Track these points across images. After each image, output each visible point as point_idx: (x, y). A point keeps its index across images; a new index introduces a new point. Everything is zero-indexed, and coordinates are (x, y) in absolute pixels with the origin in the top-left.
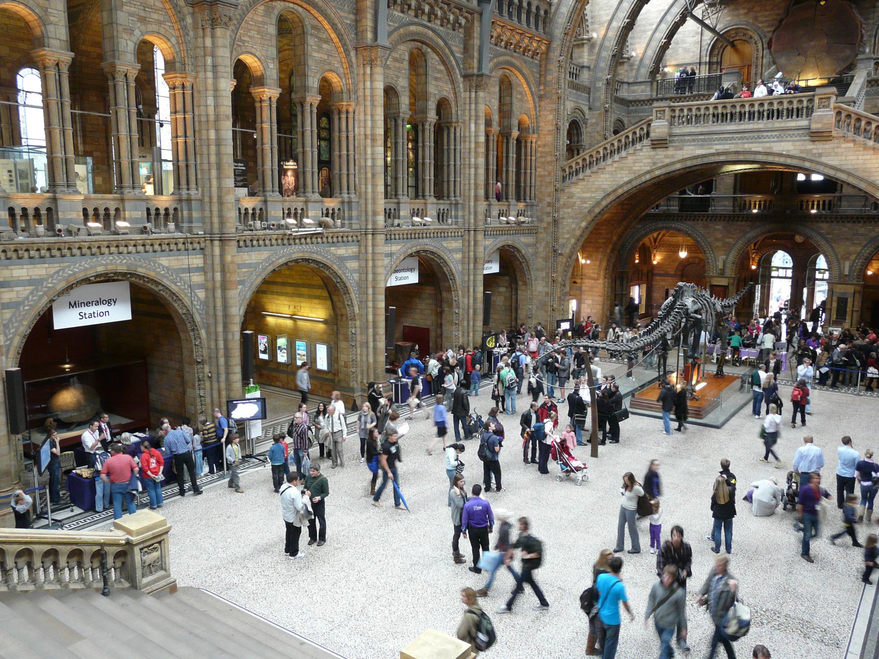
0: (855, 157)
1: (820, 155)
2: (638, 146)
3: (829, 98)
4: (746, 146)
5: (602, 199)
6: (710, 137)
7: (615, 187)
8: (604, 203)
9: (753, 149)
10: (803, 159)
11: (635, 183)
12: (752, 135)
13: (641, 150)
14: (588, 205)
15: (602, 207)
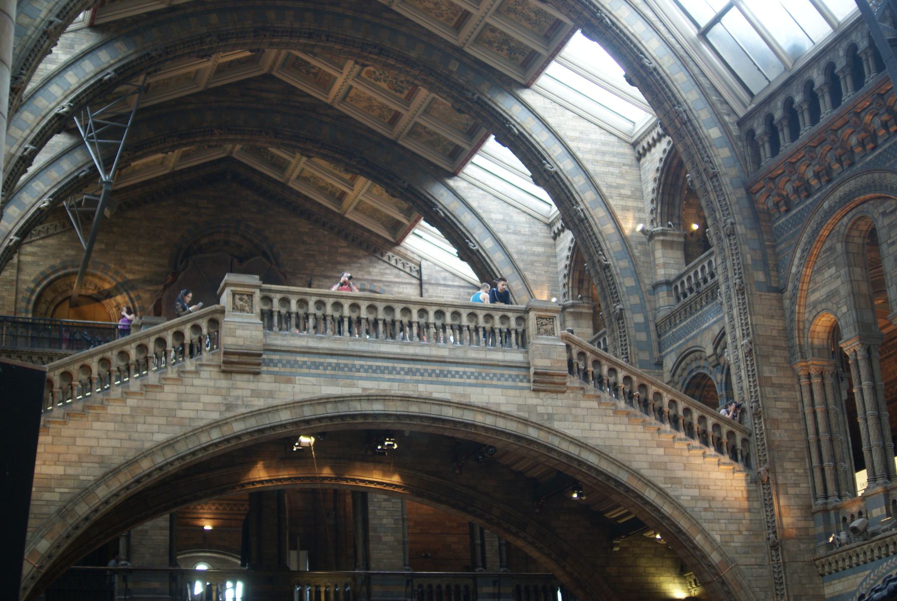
0: (603, 426)
1: (551, 417)
2: (189, 364)
3: (552, 319)
4: (423, 389)
5: (98, 482)
6: (349, 361)
7: (131, 455)
8: (102, 492)
9: (436, 395)
10: (525, 422)
11: (183, 448)
12: (430, 367)
13: (197, 372)
14: (56, 497)
15: (95, 502)
